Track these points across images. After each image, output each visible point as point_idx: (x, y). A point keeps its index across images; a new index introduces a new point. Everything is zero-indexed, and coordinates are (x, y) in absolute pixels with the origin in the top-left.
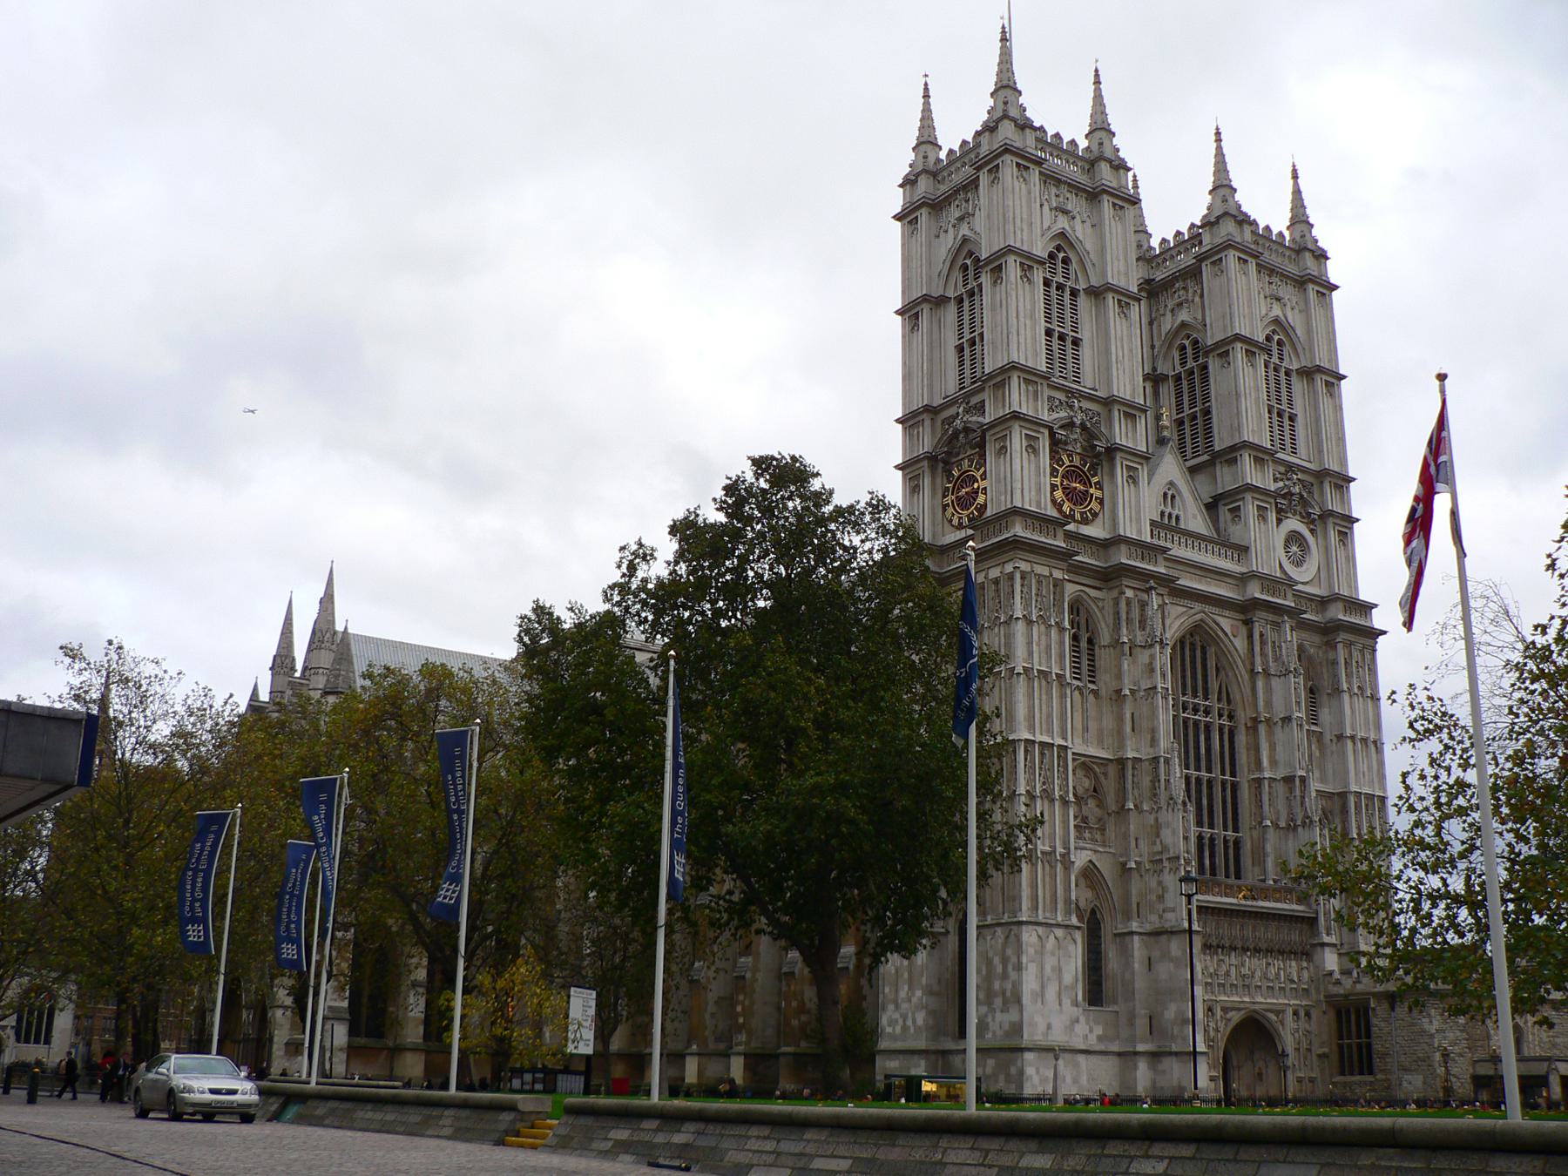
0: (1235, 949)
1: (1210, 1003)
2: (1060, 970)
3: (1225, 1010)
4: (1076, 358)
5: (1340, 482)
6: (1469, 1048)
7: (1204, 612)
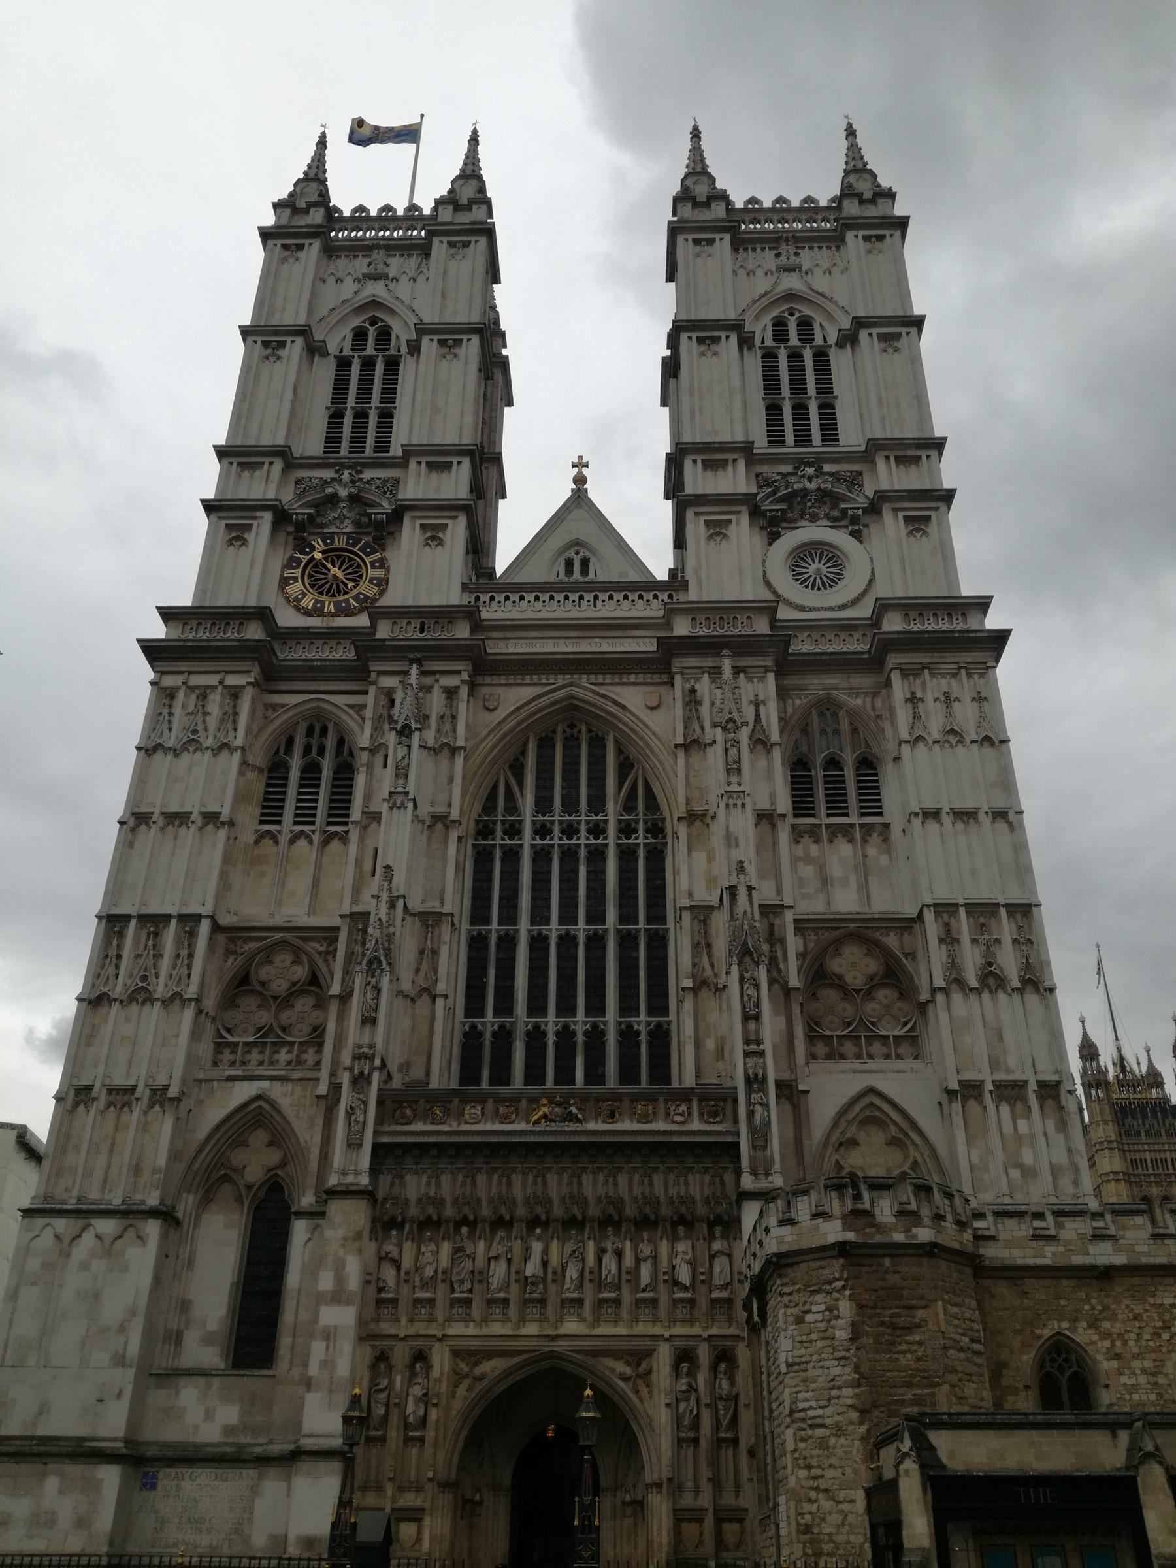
0: (500, 1223)
1: (419, 1343)
2: (97, 1296)
3: (469, 1355)
5: (910, 453)
6: (864, 1412)
7: (571, 684)
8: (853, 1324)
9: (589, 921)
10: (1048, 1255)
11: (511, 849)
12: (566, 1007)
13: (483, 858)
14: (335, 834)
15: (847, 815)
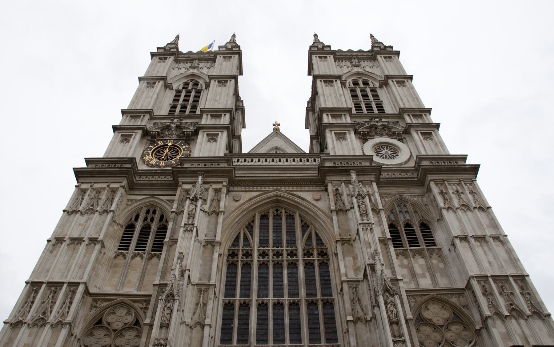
7: (277, 190)
9: (290, 296)
11: (247, 263)
13: (232, 266)
14: (155, 255)
15: (419, 246)
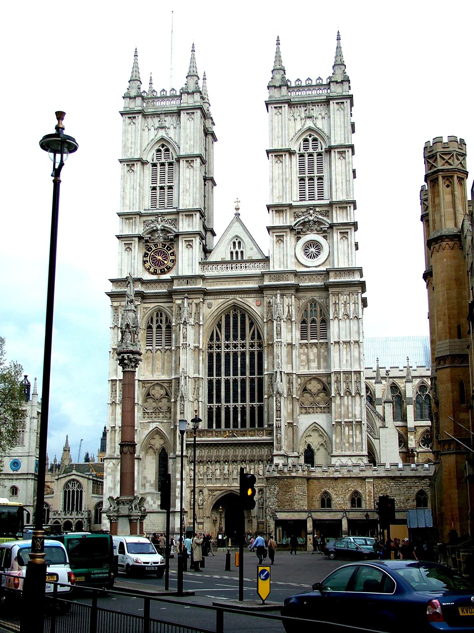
0: (217, 462)
1: (200, 488)
3: (211, 490)
4: (170, 195)
6: (279, 507)
7: (234, 299)
8: (278, 493)
10: (325, 475)
12: (235, 401)
14: (168, 349)
